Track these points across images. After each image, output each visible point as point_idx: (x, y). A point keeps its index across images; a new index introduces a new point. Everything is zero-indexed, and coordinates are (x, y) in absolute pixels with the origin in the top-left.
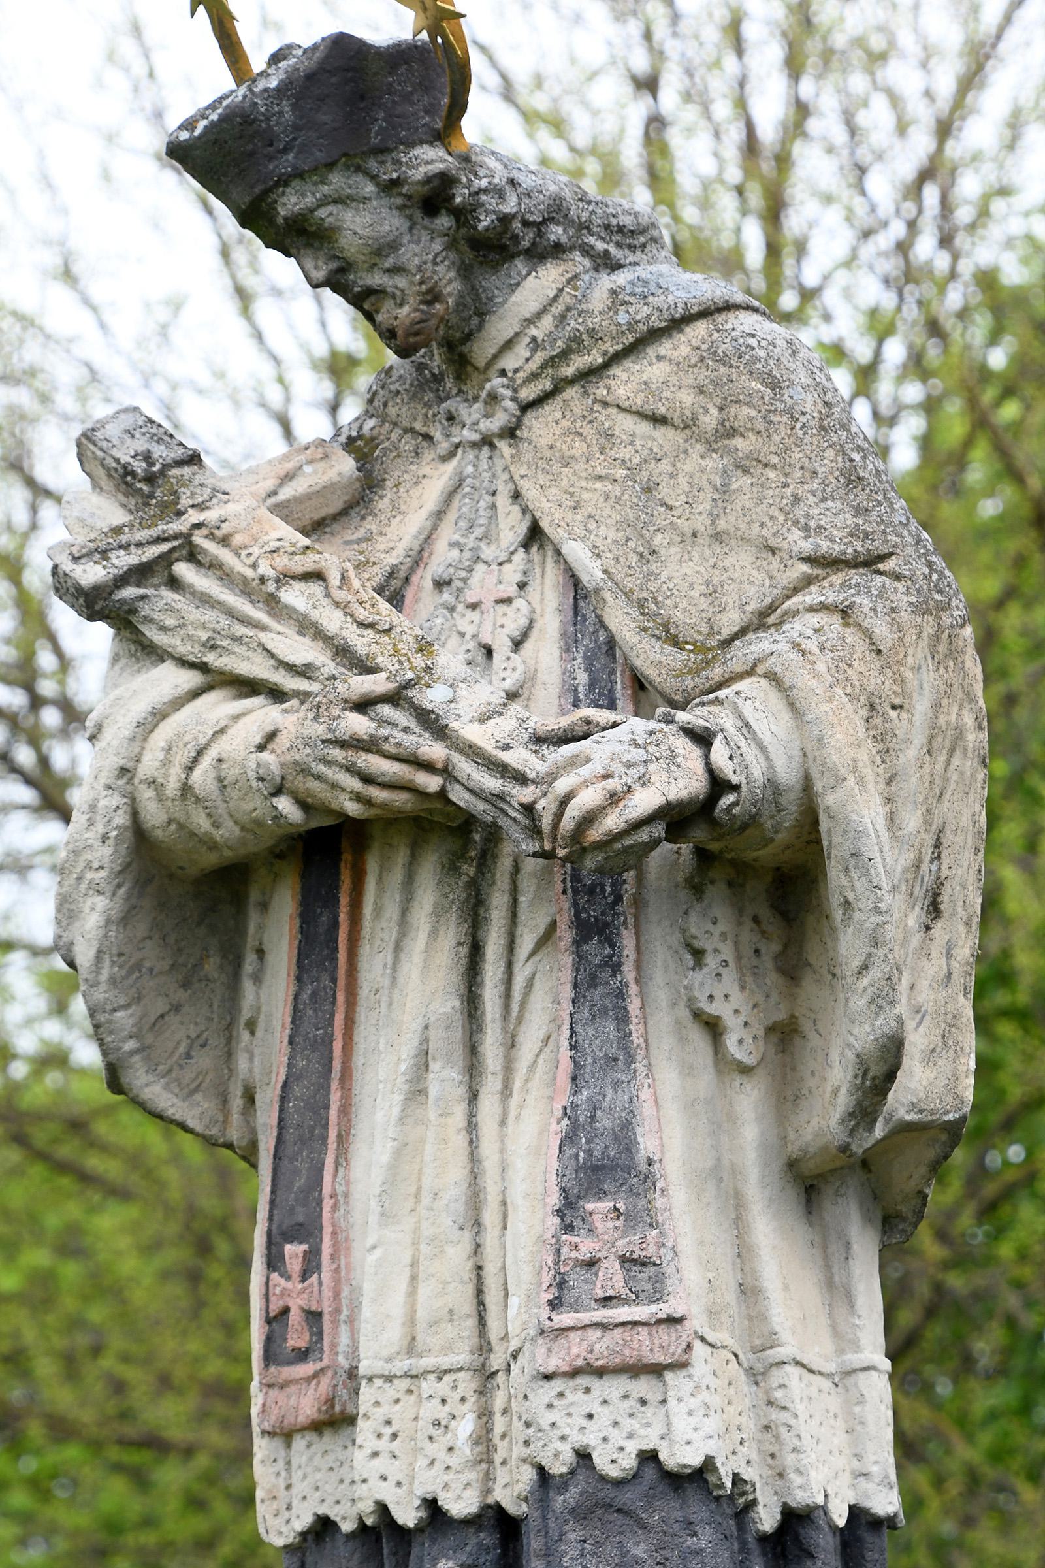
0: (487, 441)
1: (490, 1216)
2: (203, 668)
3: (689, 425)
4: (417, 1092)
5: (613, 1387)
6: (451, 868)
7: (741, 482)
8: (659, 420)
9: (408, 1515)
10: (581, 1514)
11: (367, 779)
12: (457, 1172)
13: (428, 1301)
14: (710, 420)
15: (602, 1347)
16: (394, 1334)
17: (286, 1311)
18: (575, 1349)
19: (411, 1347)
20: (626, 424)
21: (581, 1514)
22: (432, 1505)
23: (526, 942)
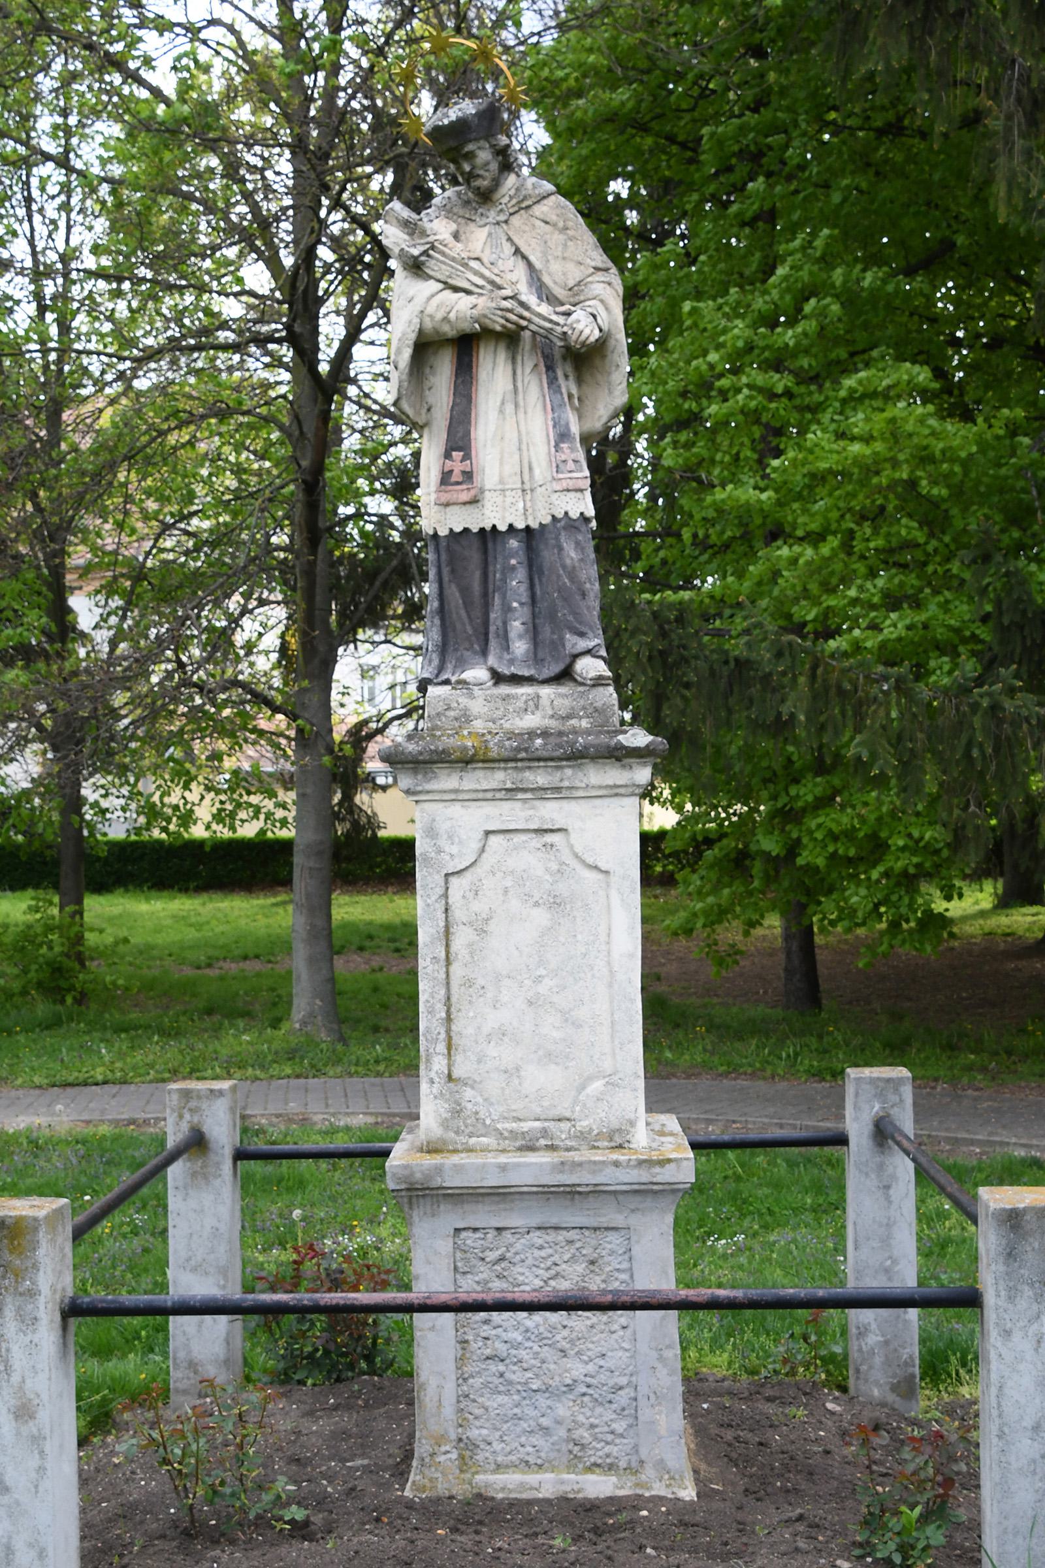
0: (498, 223)
1: (524, 447)
2: (445, 283)
3: (555, 225)
4: (501, 411)
5: (572, 494)
6: (508, 347)
7: (570, 243)
8: (547, 223)
9: (503, 528)
10: (564, 528)
11: (507, 320)
12: (516, 434)
13: (508, 470)
14: (561, 224)
15: (571, 484)
16: (496, 479)
17: (451, 471)
18: (564, 484)
19: (501, 482)
20: (538, 223)
21: (564, 528)
22: (511, 526)
23: (528, 370)
